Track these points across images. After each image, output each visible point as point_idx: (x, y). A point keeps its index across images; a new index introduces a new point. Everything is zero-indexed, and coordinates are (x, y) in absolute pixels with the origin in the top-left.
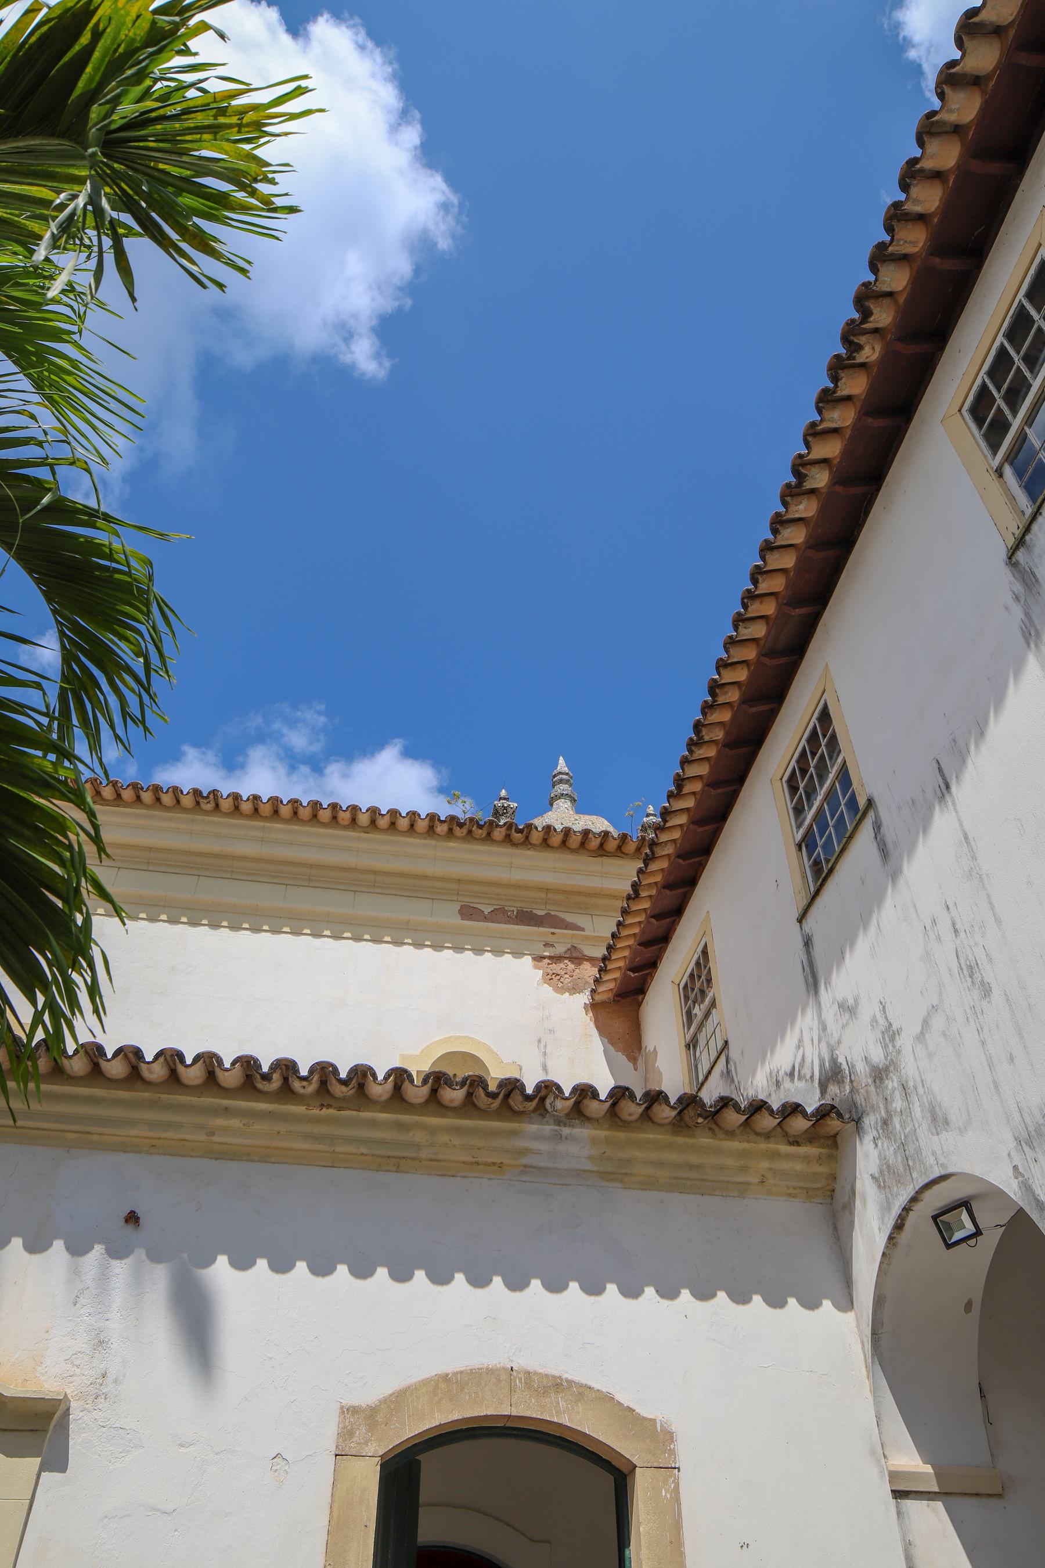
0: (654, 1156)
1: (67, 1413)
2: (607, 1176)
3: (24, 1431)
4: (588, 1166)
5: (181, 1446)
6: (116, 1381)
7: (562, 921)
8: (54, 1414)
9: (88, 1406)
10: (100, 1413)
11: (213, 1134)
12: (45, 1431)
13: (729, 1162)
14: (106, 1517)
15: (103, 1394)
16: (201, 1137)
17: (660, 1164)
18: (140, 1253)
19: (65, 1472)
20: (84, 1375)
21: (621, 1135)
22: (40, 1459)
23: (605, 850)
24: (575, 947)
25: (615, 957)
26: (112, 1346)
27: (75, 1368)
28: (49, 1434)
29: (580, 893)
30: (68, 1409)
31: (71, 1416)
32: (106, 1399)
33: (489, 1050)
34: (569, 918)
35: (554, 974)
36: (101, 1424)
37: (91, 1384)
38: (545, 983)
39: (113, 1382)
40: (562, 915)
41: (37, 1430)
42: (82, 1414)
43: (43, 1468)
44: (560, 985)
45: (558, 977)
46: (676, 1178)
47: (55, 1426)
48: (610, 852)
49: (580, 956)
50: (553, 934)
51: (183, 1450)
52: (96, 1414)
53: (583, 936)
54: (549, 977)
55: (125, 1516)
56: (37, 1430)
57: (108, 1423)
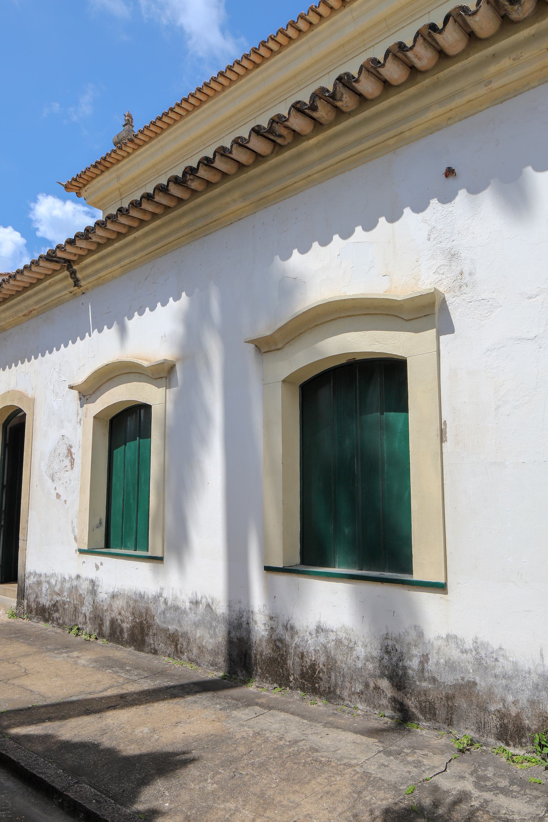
1: (444, 301)
3: (421, 317)
5: (530, 298)
6: (471, 274)
8: (434, 303)
9: (456, 294)
10: (466, 295)
11: (490, 82)
12: (433, 314)
14: (488, 350)
15: (464, 284)
16: (482, 91)
18: (462, 194)
19: (454, 333)
20: (448, 277)
22: (435, 330)
26: (461, 255)
27: (441, 275)
28: (436, 316)
30: (444, 299)
31: (447, 302)
32: (467, 286)
36: (468, 301)
37: (455, 281)
39: (469, 275)
41: (428, 315)
42: (454, 299)
43: (439, 335)
47: (439, 310)
51: (532, 300)
52: (462, 297)
55: (501, 347)
56: (428, 315)
57: (472, 299)
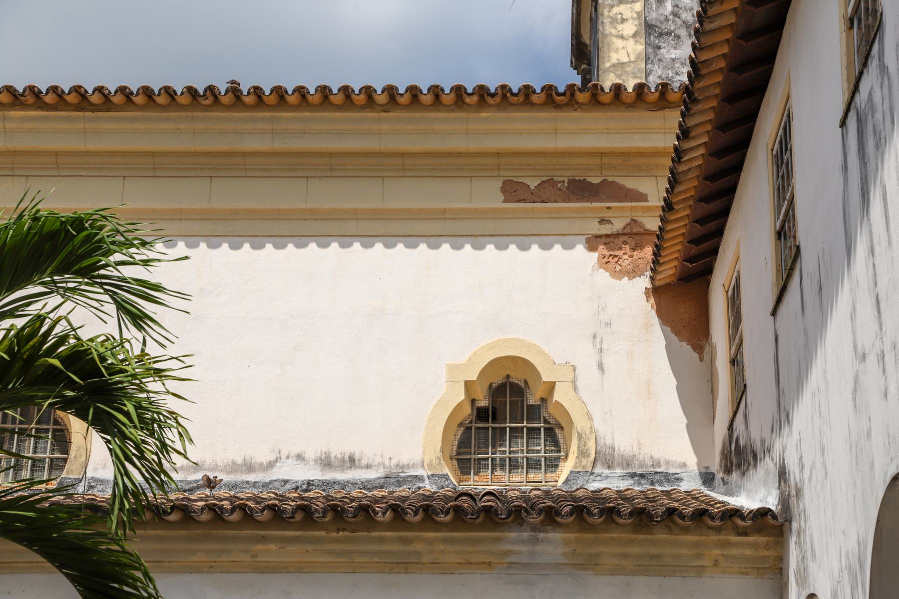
0: (618, 550)
2: (582, 566)
4: (563, 560)
7: (621, 187)
13: (685, 551)
17: (625, 556)
21: (590, 536)
23: (667, 101)
24: (635, 221)
25: (665, 254)
29: (640, 153)
33: (540, 351)
34: (630, 183)
35: (611, 255)
38: (601, 267)
40: (622, 181)
44: (618, 268)
45: (616, 259)
46: (640, 565)
48: (674, 102)
49: (642, 230)
50: (609, 208)
53: (643, 207)
54: (606, 260)
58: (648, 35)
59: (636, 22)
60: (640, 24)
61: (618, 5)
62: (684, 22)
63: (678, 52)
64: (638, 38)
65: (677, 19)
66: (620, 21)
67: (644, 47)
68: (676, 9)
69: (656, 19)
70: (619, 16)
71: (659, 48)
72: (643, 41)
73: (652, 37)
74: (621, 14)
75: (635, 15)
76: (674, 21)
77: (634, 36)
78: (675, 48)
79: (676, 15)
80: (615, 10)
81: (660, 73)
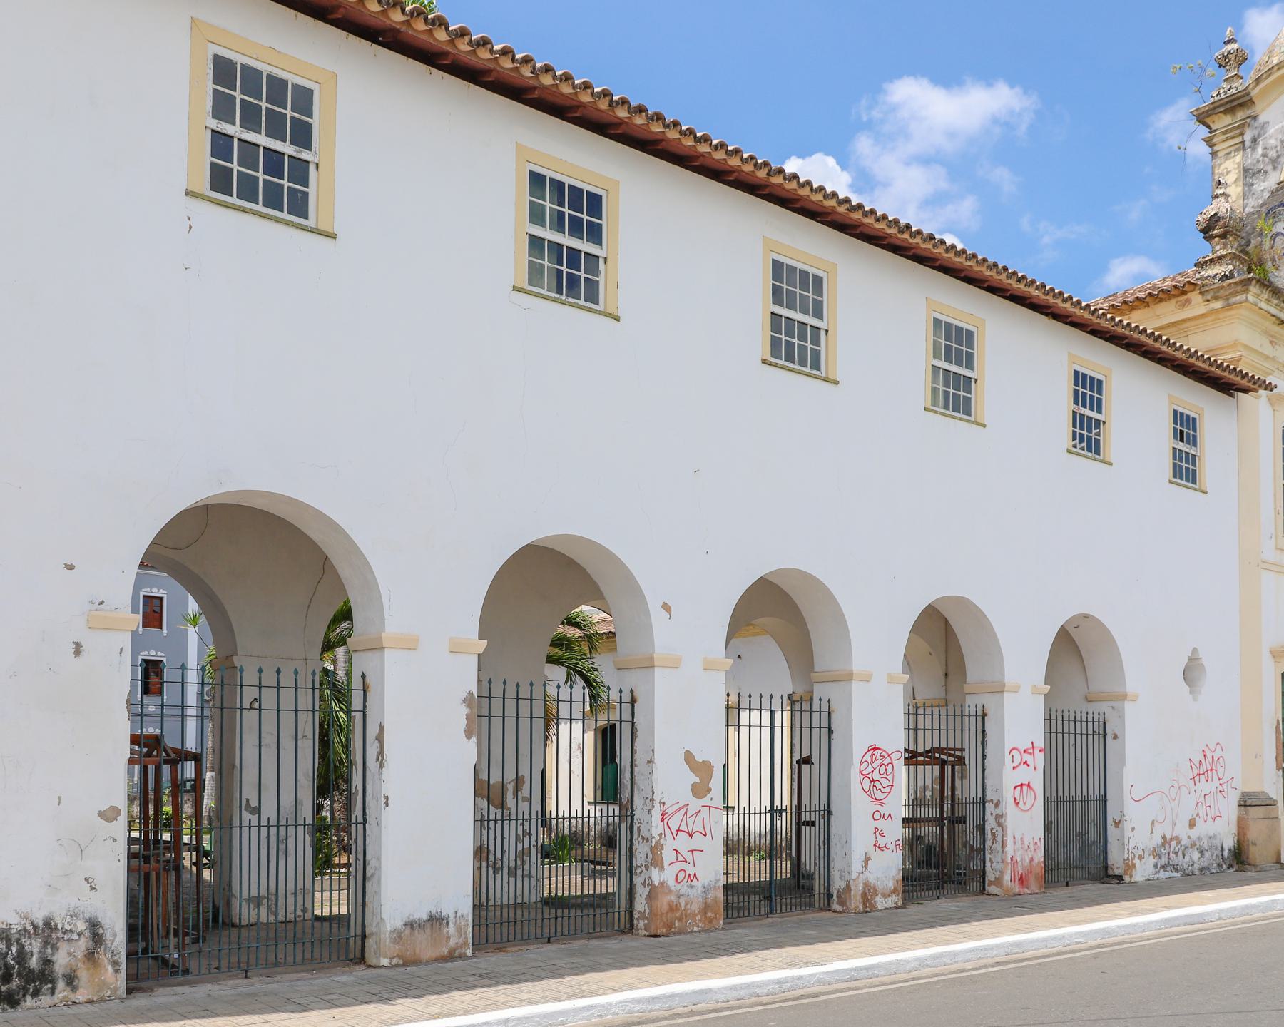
58: (1245, 177)
59: (1237, 171)
60: (1239, 172)
61: (1224, 162)
62: (1270, 159)
63: (1265, 183)
64: (1238, 183)
65: (1266, 158)
66: (1225, 174)
67: (1241, 188)
68: (1265, 151)
69: (1251, 163)
70: (1225, 170)
71: (1253, 185)
72: (1241, 182)
73: (1248, 179)
74: (1226, 168)
75: (1236, 166)
76: (1263, 161)
77: (1235, 182)
78: (1264, 182)
79: (1264, 155)
80: (1222, 167)
81: (1253, 204)
